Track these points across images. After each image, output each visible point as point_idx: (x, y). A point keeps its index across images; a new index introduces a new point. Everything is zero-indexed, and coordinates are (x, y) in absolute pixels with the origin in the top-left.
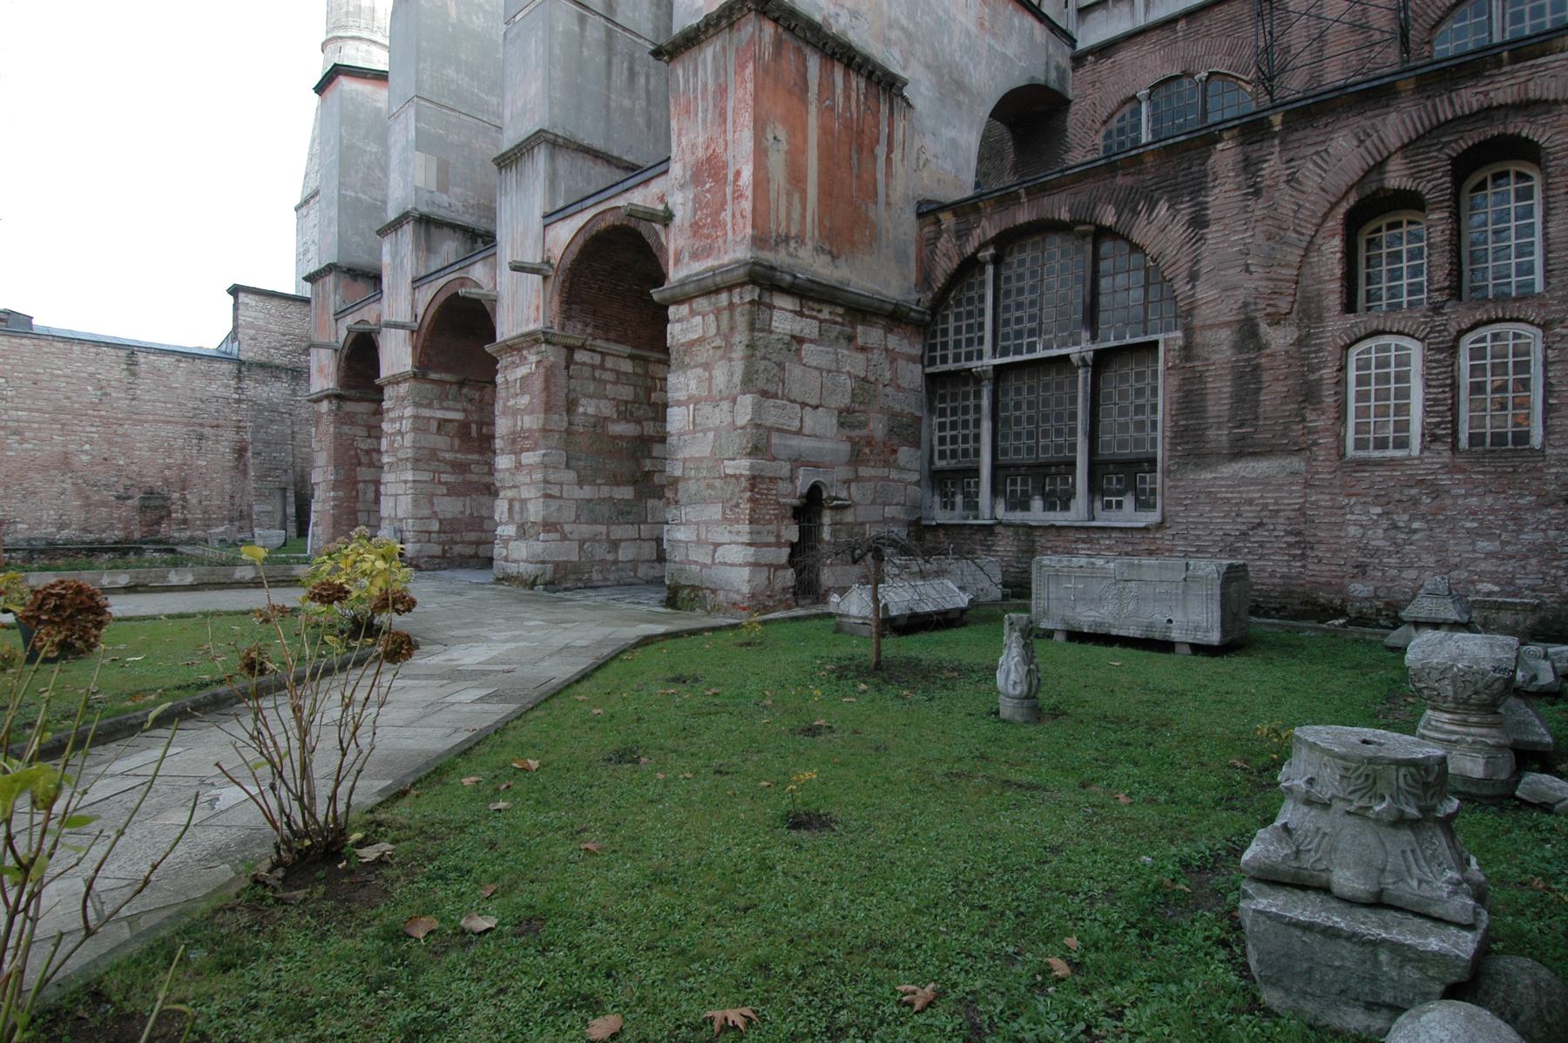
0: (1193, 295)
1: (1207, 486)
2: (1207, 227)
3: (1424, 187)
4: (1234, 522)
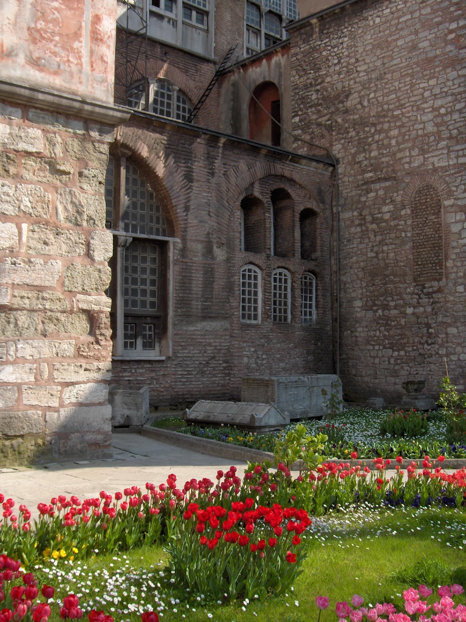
0: (186, 220)
1: (192, 335)
2: (192, 182)
3: (265, 201)
4: (203, 356)
